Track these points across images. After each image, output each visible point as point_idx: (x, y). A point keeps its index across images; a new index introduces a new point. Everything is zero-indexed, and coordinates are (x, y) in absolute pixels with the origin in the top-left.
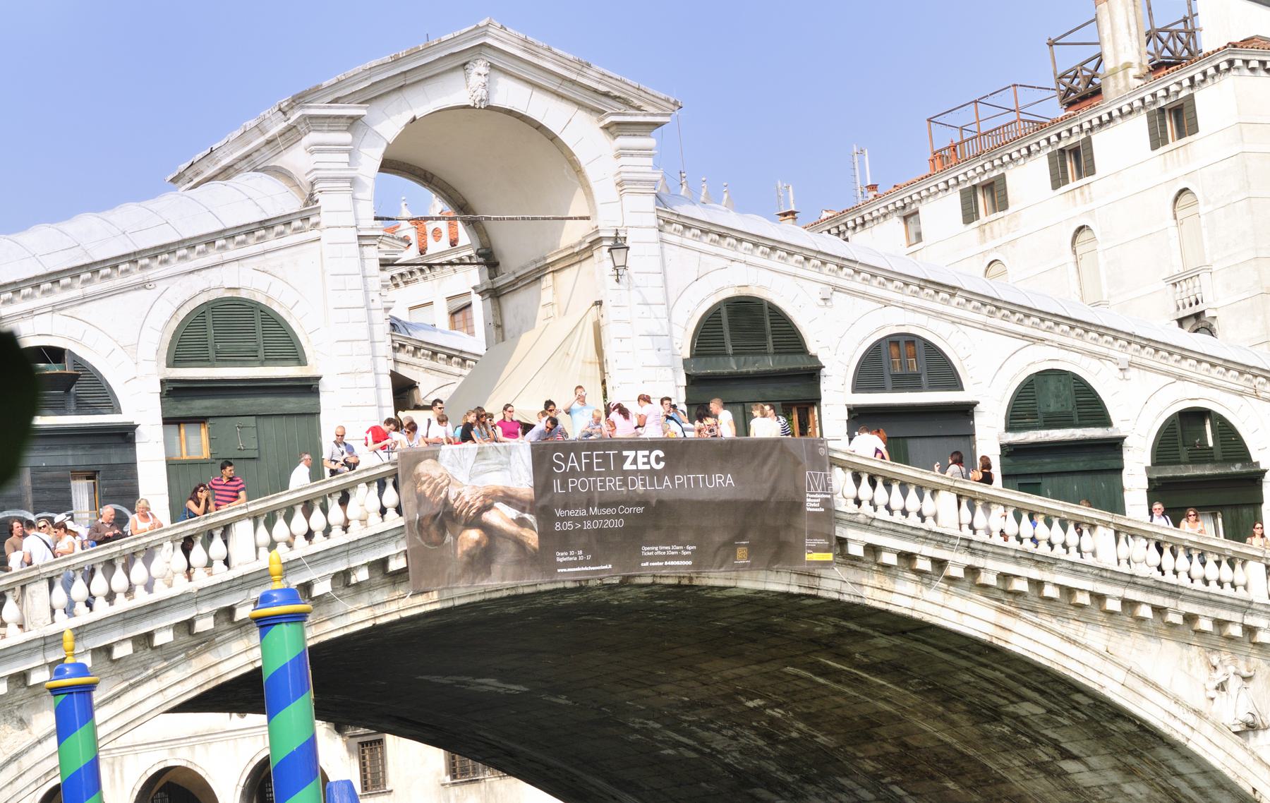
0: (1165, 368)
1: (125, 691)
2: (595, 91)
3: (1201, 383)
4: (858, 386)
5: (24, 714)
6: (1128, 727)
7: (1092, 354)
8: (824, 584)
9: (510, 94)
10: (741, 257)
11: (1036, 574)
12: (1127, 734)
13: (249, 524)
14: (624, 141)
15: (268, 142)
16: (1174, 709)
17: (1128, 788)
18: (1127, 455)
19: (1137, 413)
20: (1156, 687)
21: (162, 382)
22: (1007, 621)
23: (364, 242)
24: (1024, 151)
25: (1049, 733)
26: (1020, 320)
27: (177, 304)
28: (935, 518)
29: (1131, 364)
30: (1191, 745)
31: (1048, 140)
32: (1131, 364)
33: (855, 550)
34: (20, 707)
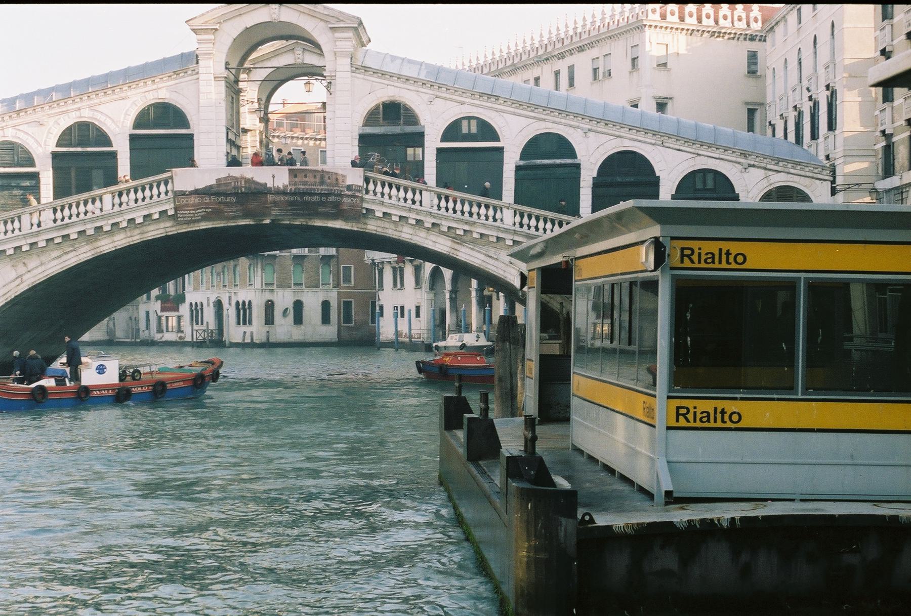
0: (610, 132)
3: (630, 139)
4: (444, 139)
7: (571, 126)
8: (369, 227)
10: (392, 83)
11: (467, 228)
14: (337, 35)
18: (584, 173)
19: (591, 152)
21: (130, 135)
26: (532, 111)
28: (421, 202)
29: (590, 130)
32: (590, 130)
33: (379, 214)
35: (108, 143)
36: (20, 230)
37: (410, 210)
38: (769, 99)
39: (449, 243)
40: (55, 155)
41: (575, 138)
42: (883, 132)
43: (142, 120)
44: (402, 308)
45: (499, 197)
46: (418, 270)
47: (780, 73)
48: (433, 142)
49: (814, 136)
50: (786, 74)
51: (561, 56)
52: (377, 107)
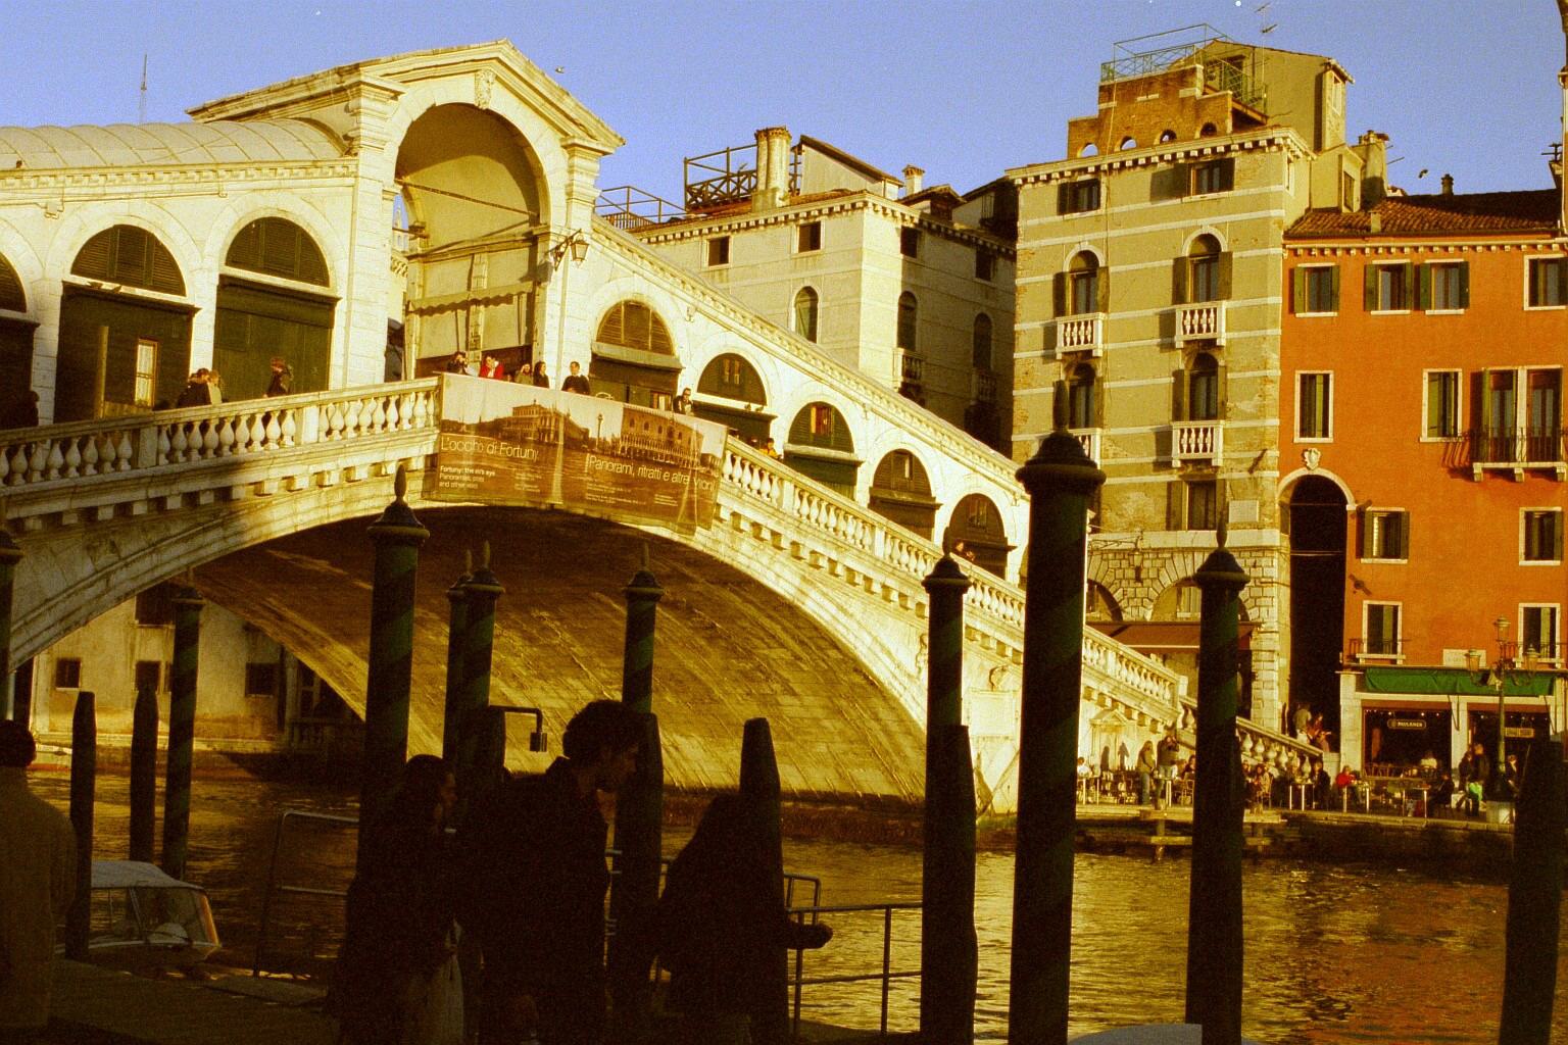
1: (198, 533)
2: (567, 116)
5: (117, 539)
6: (858, 679)
11: (834, 556)
12: (853, 686)
13: (314, 409)
15: (311, 98)
16: (897, 672)
17: (826, 723)
20: (889, 654)
21: (222, 277)
22: (805, 587)
23: (387, 196)
24: (678, 236)
25: (785, 675)
27: (241, 214)
30: (902, 701)
31: (701, 231)
34: (114, 532)
35: (180, 289)
36: (133, 462)
39: (797, 581)
52: (617, 308)
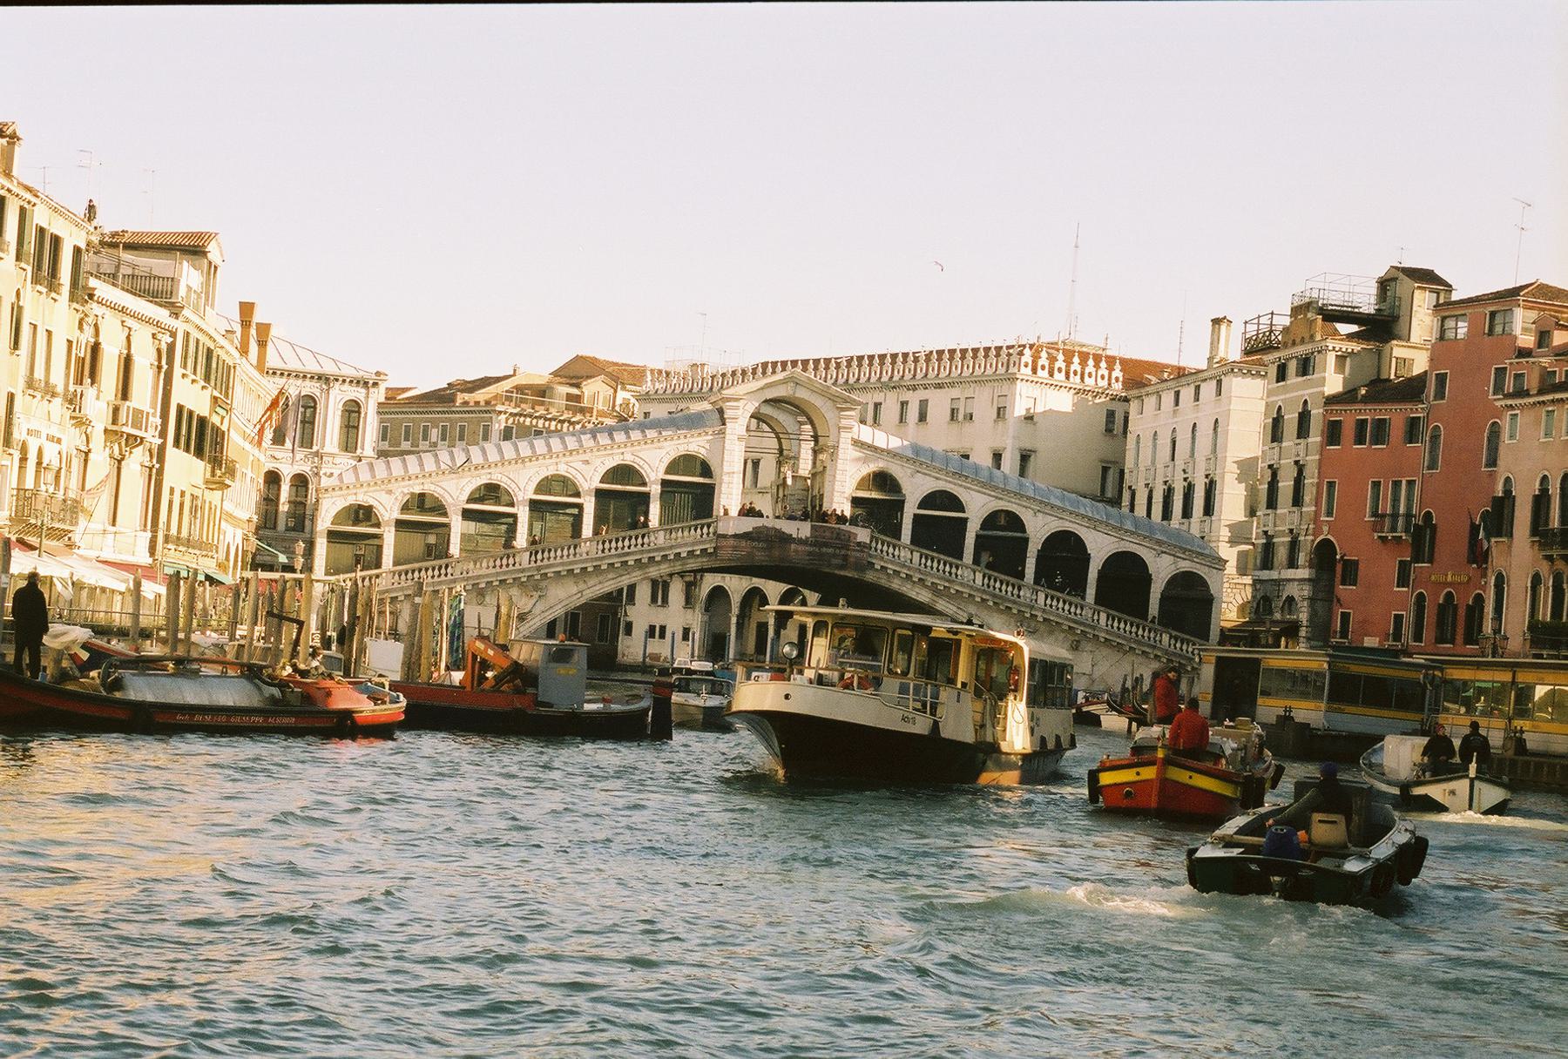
4: (920, 507)
9: (802, 394)
19: (1039, 528)
37: (904, 566)
38: (1129, 463)
40: (600, 494)
41: (1026, 516)
42: (1266, 533)
43: (673, 467)
44: (663, 629)
45: (960, 557)
46: (690, 589)
47: (1146, 443)
48: (911, 509)
49: (1187, 513)
50: (1155, 446)
51: (914, 388)
